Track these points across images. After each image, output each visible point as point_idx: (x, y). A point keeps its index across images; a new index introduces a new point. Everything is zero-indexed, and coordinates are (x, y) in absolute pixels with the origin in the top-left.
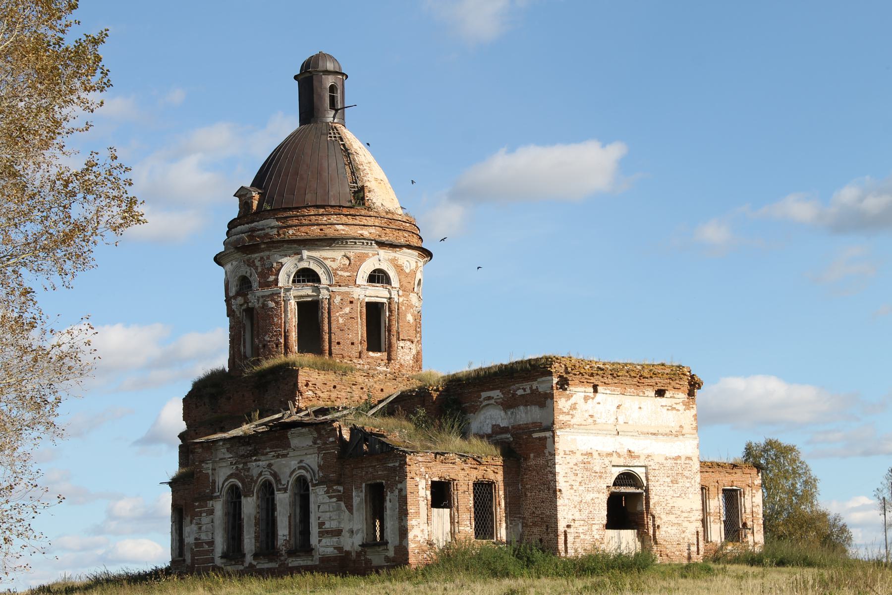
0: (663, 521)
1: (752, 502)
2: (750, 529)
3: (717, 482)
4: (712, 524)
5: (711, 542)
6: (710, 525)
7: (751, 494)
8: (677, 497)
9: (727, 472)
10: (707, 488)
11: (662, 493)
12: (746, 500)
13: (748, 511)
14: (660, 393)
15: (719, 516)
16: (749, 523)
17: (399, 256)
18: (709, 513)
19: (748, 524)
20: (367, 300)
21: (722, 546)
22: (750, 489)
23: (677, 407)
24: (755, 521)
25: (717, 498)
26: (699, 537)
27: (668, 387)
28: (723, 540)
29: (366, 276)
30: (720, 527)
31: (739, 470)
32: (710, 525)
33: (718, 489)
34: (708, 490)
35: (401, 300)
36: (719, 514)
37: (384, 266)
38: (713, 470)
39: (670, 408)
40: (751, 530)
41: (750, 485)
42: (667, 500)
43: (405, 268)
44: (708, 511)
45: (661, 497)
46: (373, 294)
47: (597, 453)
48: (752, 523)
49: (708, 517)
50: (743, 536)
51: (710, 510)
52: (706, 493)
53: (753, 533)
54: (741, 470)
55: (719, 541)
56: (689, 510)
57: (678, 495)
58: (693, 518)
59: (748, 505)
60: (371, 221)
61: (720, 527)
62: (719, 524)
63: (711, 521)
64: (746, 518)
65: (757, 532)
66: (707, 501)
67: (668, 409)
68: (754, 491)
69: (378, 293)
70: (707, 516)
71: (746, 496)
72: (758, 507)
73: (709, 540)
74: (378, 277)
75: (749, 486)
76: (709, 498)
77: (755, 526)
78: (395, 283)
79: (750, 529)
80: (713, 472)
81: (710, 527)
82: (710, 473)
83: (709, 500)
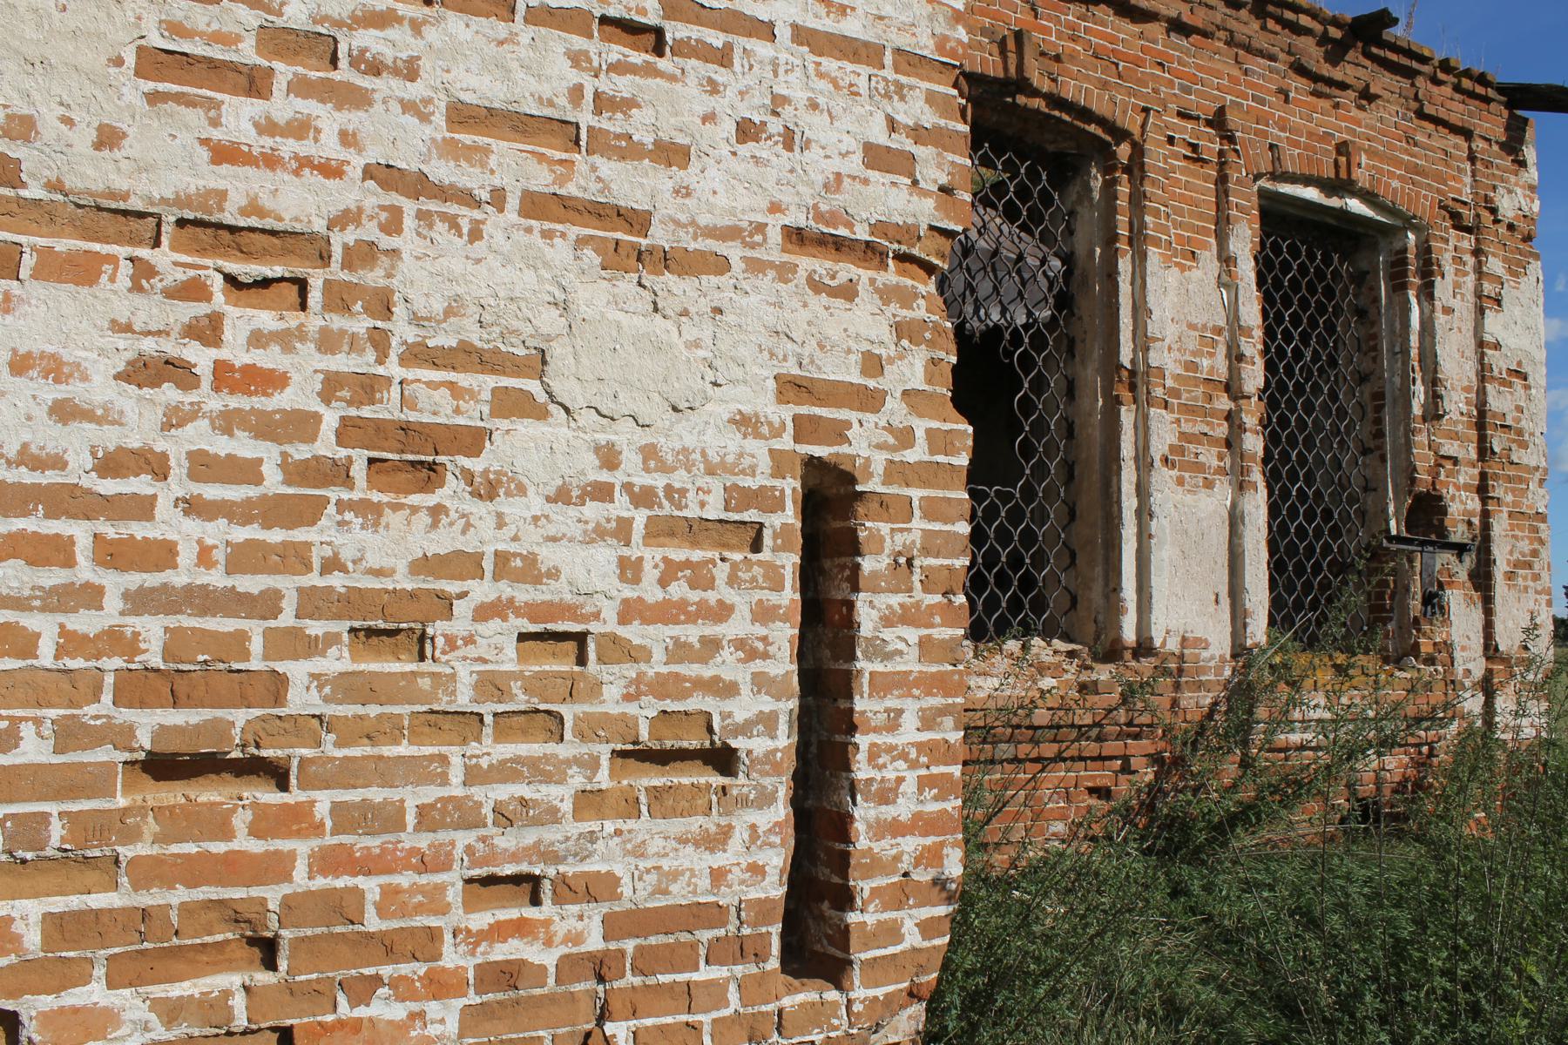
1: (1481, 344)
2: (1460, 549)
3: (1218, 121)
4: (1162, 478)
5: (1144, 648)
6: (1142, 491)
7: (1470, 280)
10: (1123, 151)
12: (1440, 319)
13: (1457, 404)
15: (1229, 417)
16: (1461, 505)
18: (1138, 379)
19: (1454, 509)
21: (1242, 693)
22: (1468, 242)
24: (1499, 490)
25: (1209, 257)
26: (868, 613)
28: (1258, 630)
30: (1235, 520)
32: (1142, 491)
33: (1222, 180)
34: (1136, 168)
36: (1224, 403)
40: (1469, 560)
41: (1468, 215)
44: (1126, 356)
48: (1474, 504)
49: (1127, 416)
50: (1415, 605)
51: (1143, 342)
52: (1110, 210)
53: (1482, 580)
54: (1405, 83)
55: (1219, 643)
59: (1456, 365)
61: (1235, 520)
62: (1223, 493)
63: (1158, 448)
64: (1442, 459)
65: (1510, 576)
66: (1124, 265)
68: (1495, 265)
70: (1114, 403)
71: (1443, 289)
72: (1517, 381)
73: (1129, 634)
75: (1459, 227)
76: (1138, 238)
77: (1500, 526)
79: (1460, 549)
81: (1144, 513)
82: (1156, 29)
83: (1140, 258)
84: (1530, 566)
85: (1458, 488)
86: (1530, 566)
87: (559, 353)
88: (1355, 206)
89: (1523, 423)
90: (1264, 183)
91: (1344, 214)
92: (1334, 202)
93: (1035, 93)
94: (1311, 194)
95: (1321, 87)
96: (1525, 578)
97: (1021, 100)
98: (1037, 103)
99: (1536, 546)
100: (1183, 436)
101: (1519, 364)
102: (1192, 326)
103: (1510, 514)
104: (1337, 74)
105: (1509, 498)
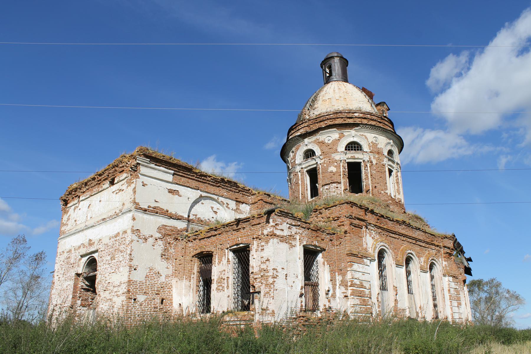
0: (101, 298)
8: (113, 273)
9: (234, 230)
11: (104, 271)
14: (112, 183)
17: (320, 136)
20: (306, 170)
23: (122, 188)
27: (116, 174)
29: (302, 157)
31: (246, 223)
35: (323, 161)
37: (310, 147)
38: (220, 232)
39: (118, 191)
42: (106, 277)
43: (326, 141)
45: (103, 276)
46: (307, 165)
47: (74, 248)
54: (248, 223)
56: (119, 284)
57: (113, 271)
58: (121, 292)
60: (302, 126)
67: (117, 193)
69: (311, 163)
72: (267, 262)
74: (310, 154)
78: (318, 152)
80: (219, 234)
82: (218, 236)
84: (269, 293)
85: (257, 283)
86: (269, 293)
87: (116, 302)
88: (241, 245)
89: (268, 269)
90: (230, 249)
91: (240, 247)
92: (239, 246)
93: (204, 252)
94: (235, 247)
95: (237, 231)
96: (268, 295)
97: (204, 253)
98: (205, 252)
99: (270, 289)
100: (218, 286)
101: (268, 258)
102: (219, 272)
103: (265, 285)
104: (238, 228)
105: (265, 282)
